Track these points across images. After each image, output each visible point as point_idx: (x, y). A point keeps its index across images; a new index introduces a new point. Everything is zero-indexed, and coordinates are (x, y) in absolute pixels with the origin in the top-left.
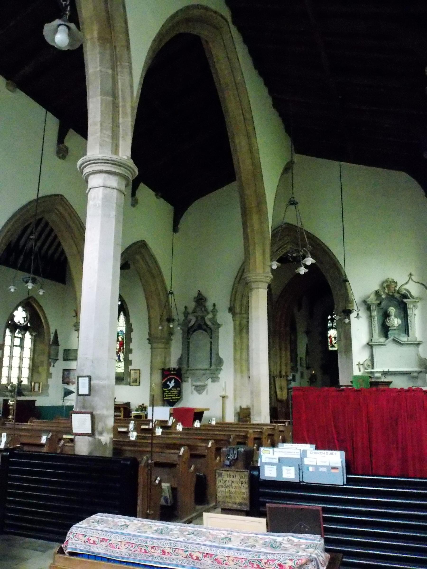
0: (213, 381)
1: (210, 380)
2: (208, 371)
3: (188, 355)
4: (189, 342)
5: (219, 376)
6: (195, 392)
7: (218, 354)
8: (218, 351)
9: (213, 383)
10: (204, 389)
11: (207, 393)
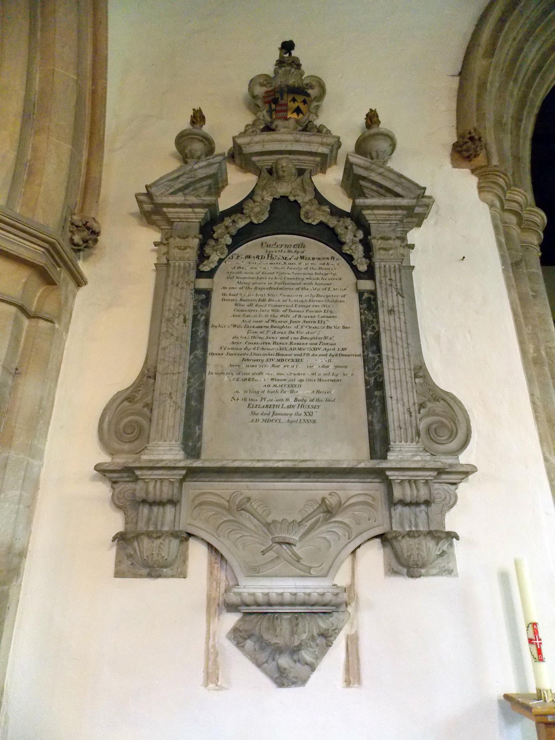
0: (406, 566)
1: (373, 557)
2: (353, 489)
3: (198, 367)
4: (204, 298)
5: (452, 521)
6: (241, 667)
7: (420, 371)
8: (419, 353)
9: (403, 583)
10: (327, 637)
11: (352, 675)
